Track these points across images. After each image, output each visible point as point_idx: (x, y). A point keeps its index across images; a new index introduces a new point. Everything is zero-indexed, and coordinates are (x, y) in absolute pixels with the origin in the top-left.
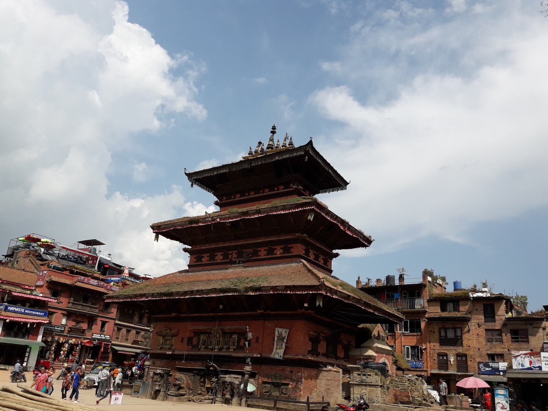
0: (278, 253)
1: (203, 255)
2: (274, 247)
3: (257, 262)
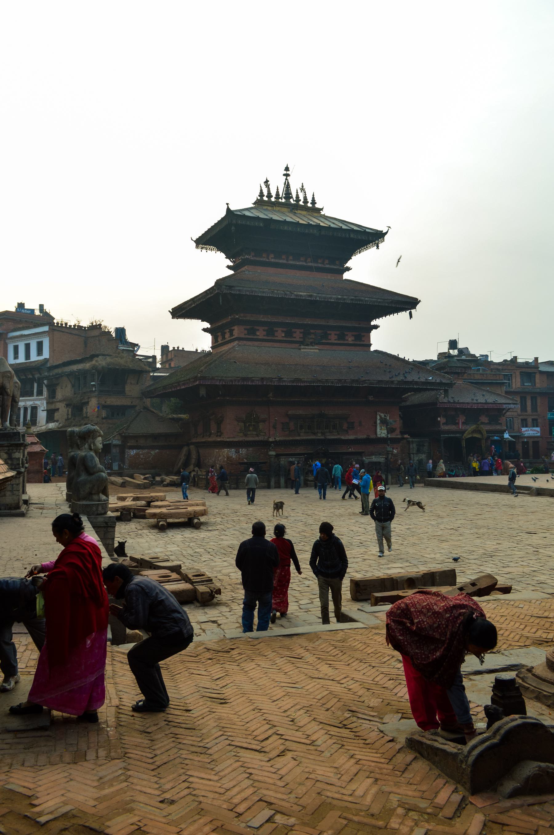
0: (350, 339)
1: (257, 328)
2: (346, 333)
3: (328, 346)
